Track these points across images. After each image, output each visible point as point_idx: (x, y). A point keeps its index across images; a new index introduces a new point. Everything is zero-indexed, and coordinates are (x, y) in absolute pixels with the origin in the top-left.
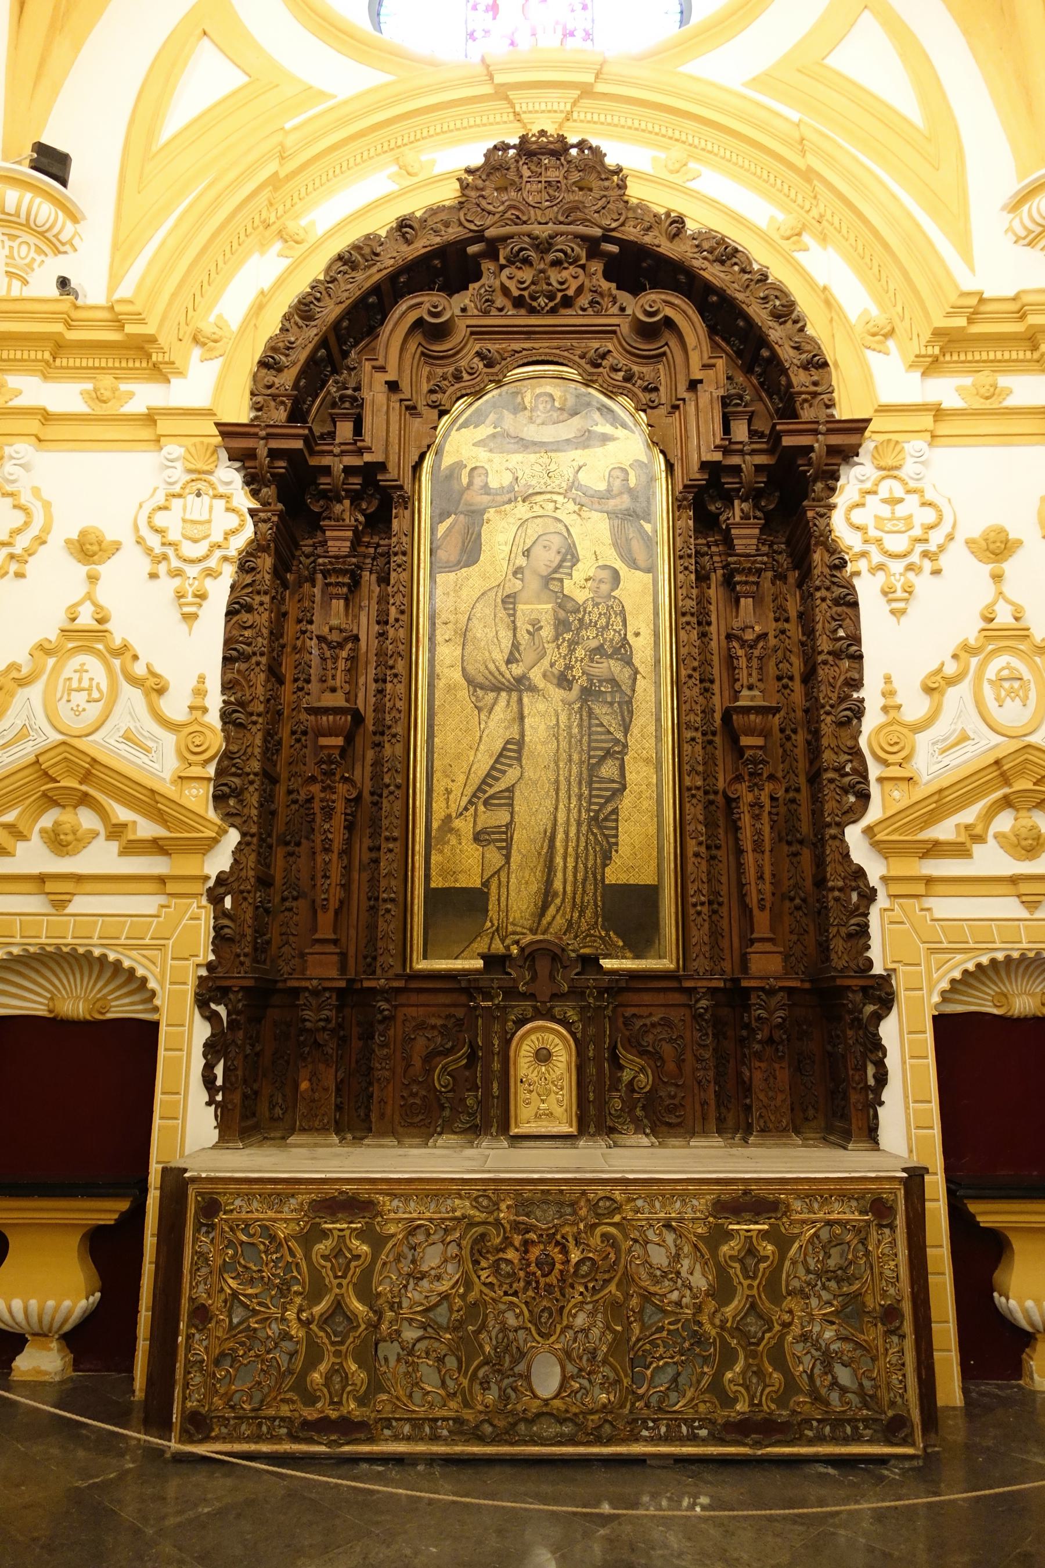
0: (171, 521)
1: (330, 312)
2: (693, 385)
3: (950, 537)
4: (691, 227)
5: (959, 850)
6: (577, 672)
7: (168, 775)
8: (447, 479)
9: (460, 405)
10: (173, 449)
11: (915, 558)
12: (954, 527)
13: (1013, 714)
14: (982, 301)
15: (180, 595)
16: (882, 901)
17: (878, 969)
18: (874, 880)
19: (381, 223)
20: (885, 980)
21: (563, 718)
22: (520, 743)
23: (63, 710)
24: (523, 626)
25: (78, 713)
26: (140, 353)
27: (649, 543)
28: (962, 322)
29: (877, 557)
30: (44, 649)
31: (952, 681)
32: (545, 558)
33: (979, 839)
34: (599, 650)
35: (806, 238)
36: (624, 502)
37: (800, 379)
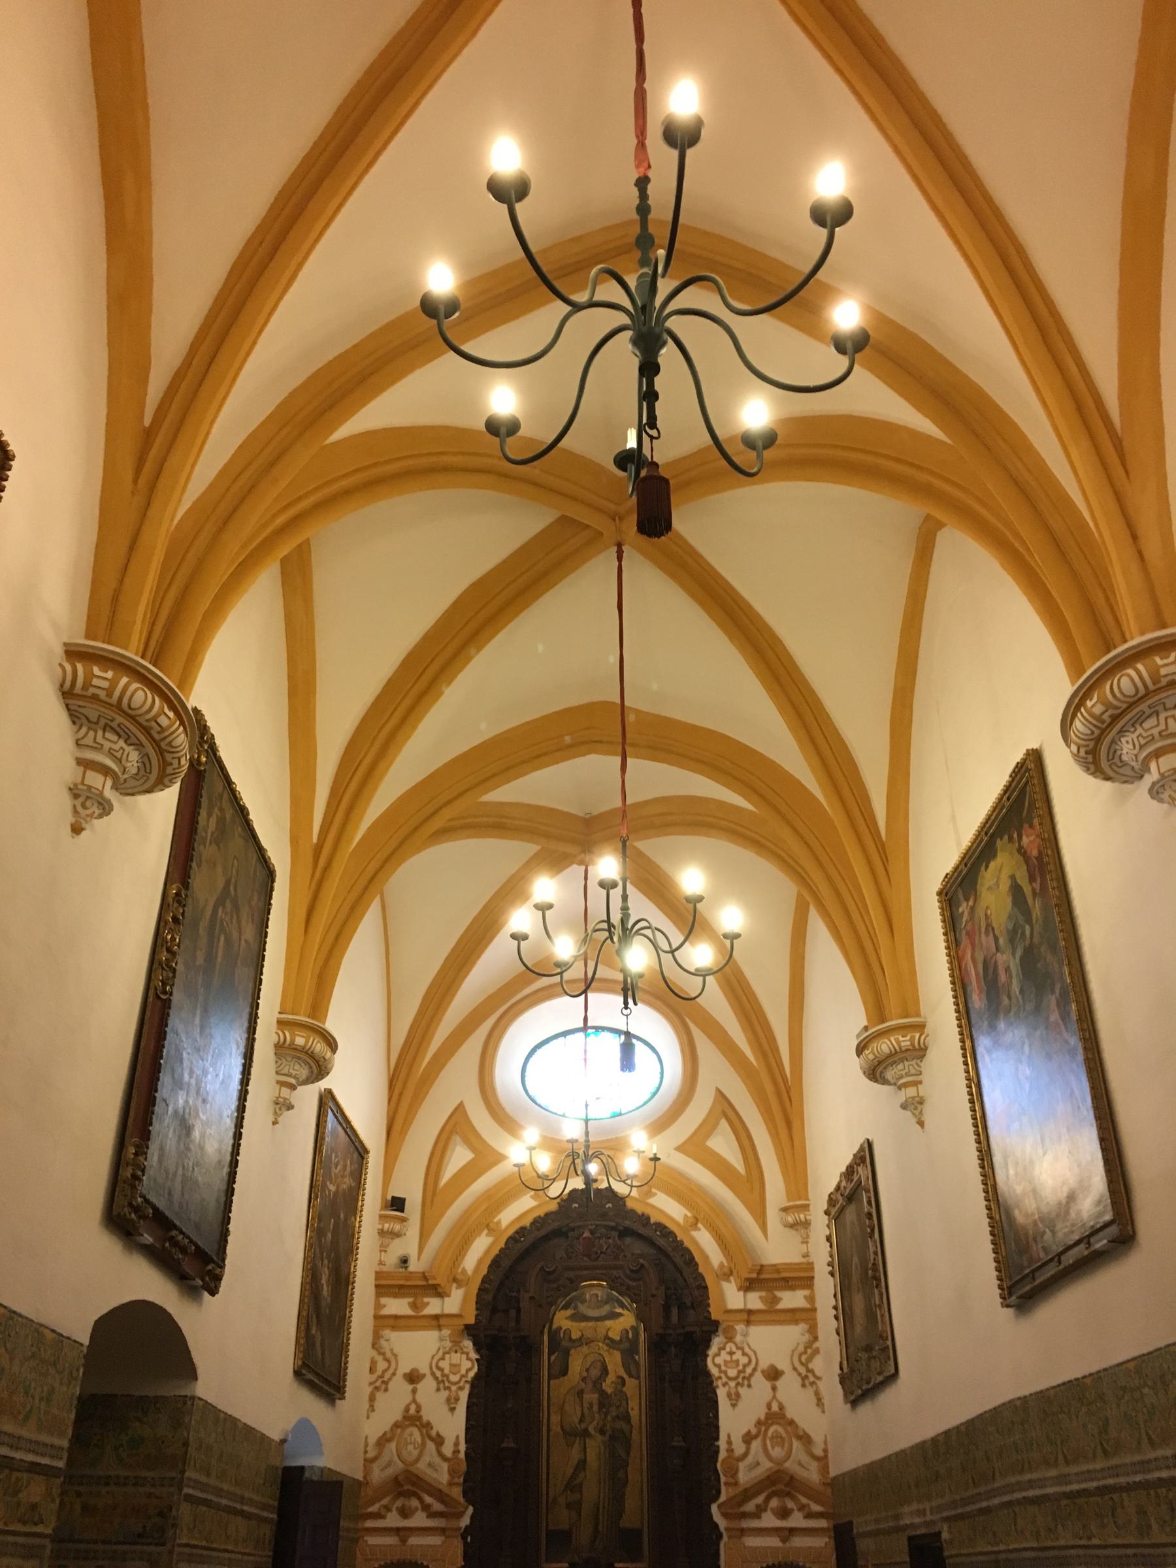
0: (445, 1365)
1: (506, 1264)
2: (653, 1296)
3: (755, 1370)
4: (652, 1221)
5: (757, 1515)
6: (608, 1428)
7: (445, 1482)
8: (554, 1336)
9: (560, 1300)
10: (446, 1332)
11: (740, 1380)
13: (777, 1452)
14: (762, 1266)
15: (448, 1400)
16: (725, 1538)
18: (722, 1528)
19: (527, 1222)
22: (585, 1461)
23: (404, 1453)
24: (586, 1405)
25: (411, 1452)
26: (437, 1291)
27: (637, 1364)
28: (754, 1275)
29: (724, 1379)
30: (396, 1425)
31: (756, 1437)
32: (595, 1373)
33: (765, 1510)
34: (617, 1417)
35: (700, 1225)
36: (626, 1345)
37: (696, 1292)
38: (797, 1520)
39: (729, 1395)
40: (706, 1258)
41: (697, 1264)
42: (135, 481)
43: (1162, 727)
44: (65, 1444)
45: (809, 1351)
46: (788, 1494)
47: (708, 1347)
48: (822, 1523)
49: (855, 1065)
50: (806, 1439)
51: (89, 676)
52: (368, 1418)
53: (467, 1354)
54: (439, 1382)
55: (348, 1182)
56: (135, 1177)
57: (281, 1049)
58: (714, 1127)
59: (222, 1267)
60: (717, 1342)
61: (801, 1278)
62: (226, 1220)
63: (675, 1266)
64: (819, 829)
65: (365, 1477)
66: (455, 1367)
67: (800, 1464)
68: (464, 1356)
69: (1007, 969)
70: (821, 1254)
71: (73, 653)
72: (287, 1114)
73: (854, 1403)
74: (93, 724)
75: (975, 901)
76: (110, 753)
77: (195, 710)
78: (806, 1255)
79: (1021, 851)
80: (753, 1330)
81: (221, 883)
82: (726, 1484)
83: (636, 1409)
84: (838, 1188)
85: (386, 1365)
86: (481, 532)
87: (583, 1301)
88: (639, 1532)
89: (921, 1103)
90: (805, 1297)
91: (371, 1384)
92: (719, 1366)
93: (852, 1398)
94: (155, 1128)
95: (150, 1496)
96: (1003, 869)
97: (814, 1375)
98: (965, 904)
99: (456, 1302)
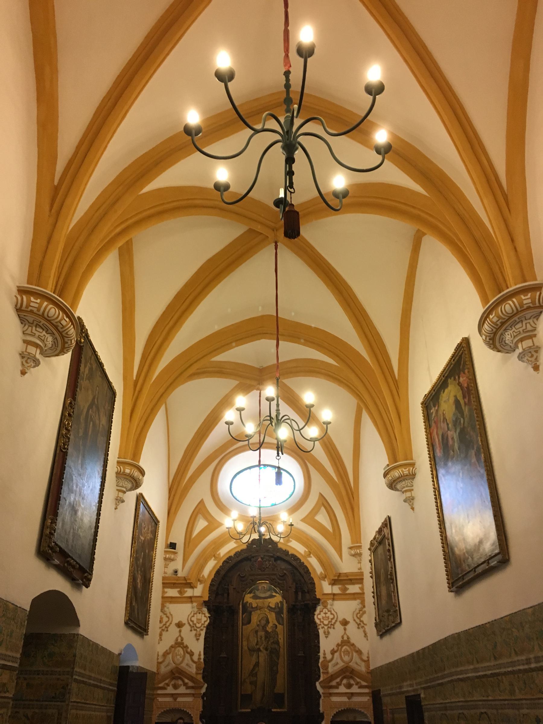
0: (194, 619)
1: (223, 573)
3: (336, 621)
4: (290, 553)
5: (337, 687)
7: (194, 672)
8: (244, 606)
10: (195, 604)
11: (329, 626)
12: (337, 618)
13: (346, 658)
14: (340, 574)
15: (196, 635)
16: (322, 698)
17: (321, 712)
19: (232, 554)
20: (323, 714)
21: (266, 657)
23: (176, 659)
24: (259, 637)
25: (179, 659)
27: (283, 618)
28: (336, 578)
29: (322, 625)
30: (172, 647)
31: (336, 652)
32: (263, 622)
33: (340, 685)
34: (273, 642)
35: (311, 555)
36: (277, 610)
38: (355, 689)
39: (324, 632)
40: (314, 570)
41: (310, 573)
42: (51, 210)
43: (524, 327)
44: (19, 656)
45: (361, 612)
46: (351, 677)
47: (315, 610)
48: (366, 691)
49: (382, 483)
50: (359, 652)
51: (29, 301)
52: (159, 643)
53: (204, 614)
54: (192, 627)
55: (150, 536)
56: (51, 534)
57: (119, 475)
58: (319, 509)
59: (91, 574)
60: (319, 608)
61: (358, 579)
62: (93, 553)
63: (300, 573)
64: (367, 374)
65: (157, 671)
66: (199, 620)
67: (357, 663)
68: (203, 615)
69: (453, 438)
70: (367, 568)
71: (22, 291)
72: (121, 505)
73: (382, 636)
74: (31, 324)
75: (438, 407)
76: (39, 338)
77: (79, 318)
78: (360, 569)
79: (460, 384)
80: (336, 602)
81: (90, 398)
82: (323, 673)
83: (282, 638)
84: (375, 538)
85: (167, 619)
86: (212, 236)
87: (258, 590)
88: (283, 695)
89: (413, 499)
90: (360, 588)
91: (160, 628)
92: (320, 619)
93: (381, 633)
94: (60, 511)
95: (58, 679)
96: (451, 392)
97: (363, 623)
98: (433, 408)
99: (200, 591)
